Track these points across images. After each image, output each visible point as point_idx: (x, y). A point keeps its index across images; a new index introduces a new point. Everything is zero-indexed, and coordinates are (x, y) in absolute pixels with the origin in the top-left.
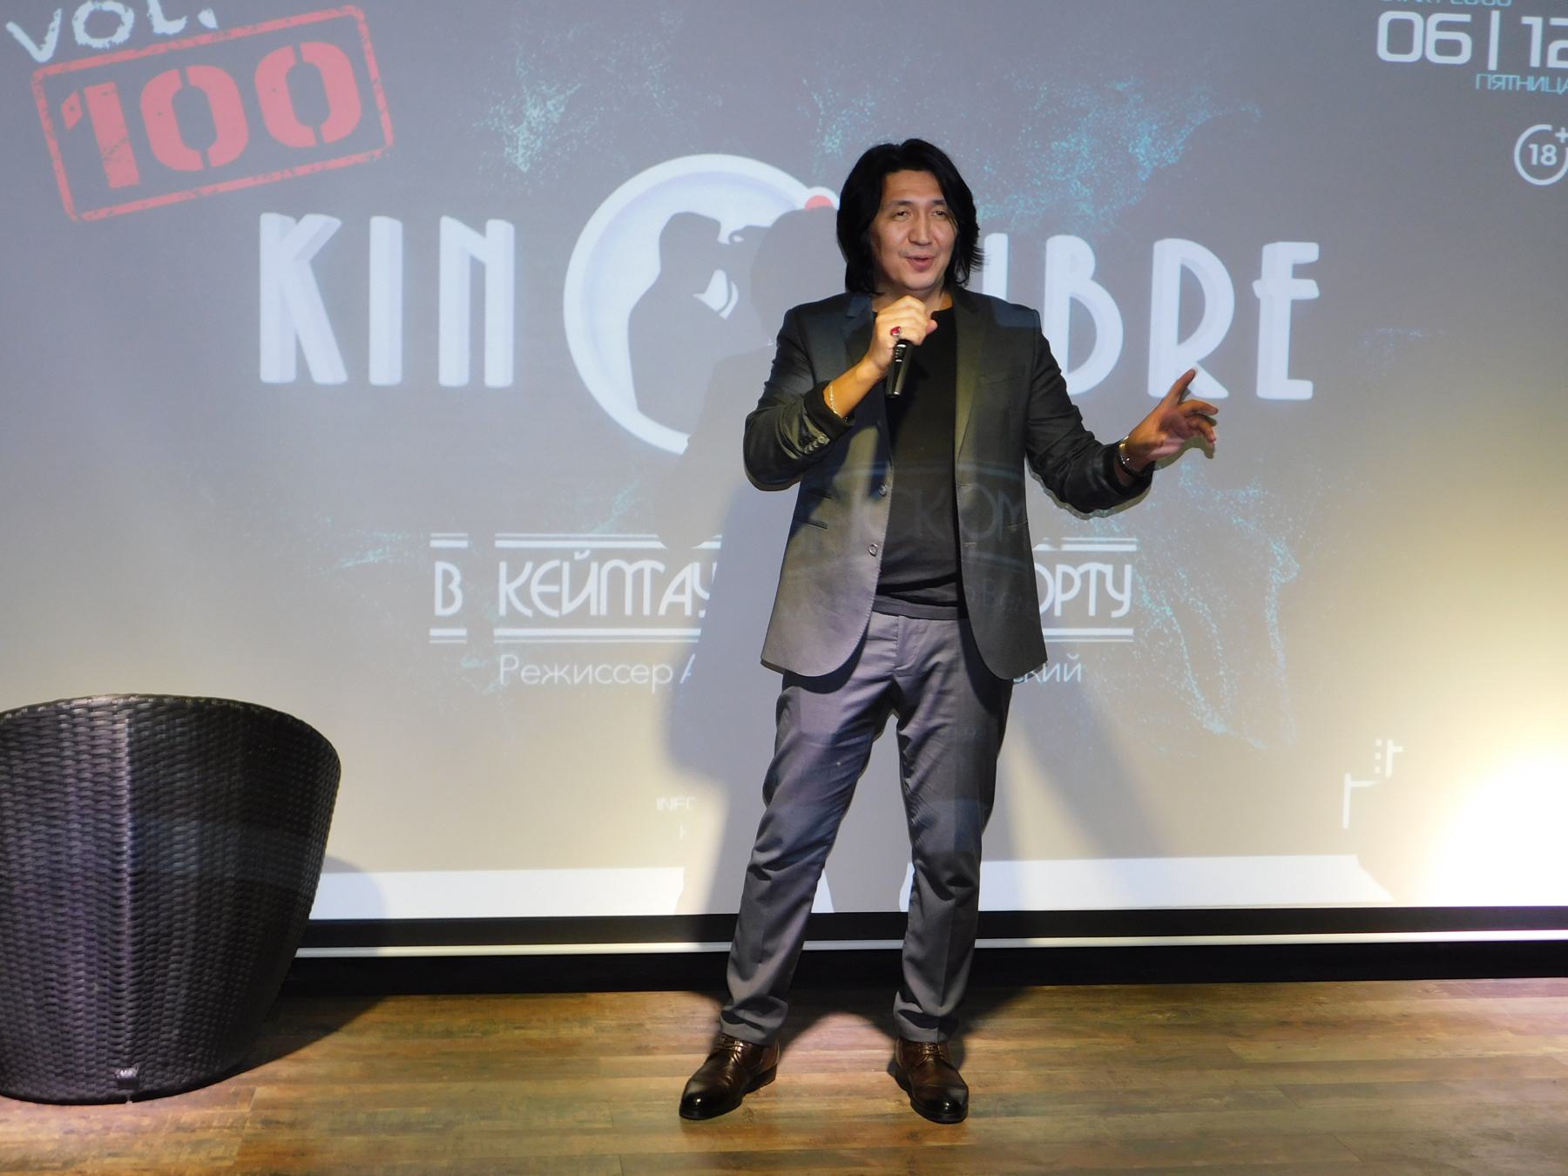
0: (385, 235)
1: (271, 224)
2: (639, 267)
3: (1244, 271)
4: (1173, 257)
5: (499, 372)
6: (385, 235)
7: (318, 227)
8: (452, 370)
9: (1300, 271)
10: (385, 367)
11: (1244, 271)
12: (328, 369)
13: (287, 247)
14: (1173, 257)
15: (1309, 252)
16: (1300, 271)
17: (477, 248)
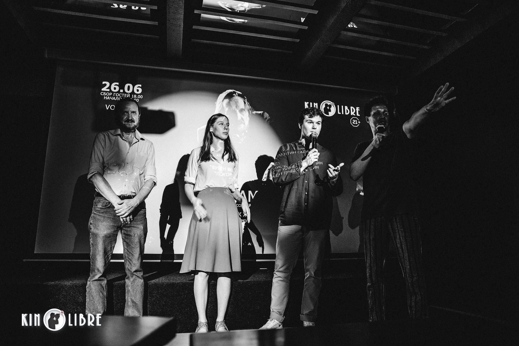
0: (311, 103)
2: (324, 106)
3: (356, 109)
4: (351, 107)
6: (311, 103)
7: (308, 103)
11: (356, 109)
14: (351, 107)
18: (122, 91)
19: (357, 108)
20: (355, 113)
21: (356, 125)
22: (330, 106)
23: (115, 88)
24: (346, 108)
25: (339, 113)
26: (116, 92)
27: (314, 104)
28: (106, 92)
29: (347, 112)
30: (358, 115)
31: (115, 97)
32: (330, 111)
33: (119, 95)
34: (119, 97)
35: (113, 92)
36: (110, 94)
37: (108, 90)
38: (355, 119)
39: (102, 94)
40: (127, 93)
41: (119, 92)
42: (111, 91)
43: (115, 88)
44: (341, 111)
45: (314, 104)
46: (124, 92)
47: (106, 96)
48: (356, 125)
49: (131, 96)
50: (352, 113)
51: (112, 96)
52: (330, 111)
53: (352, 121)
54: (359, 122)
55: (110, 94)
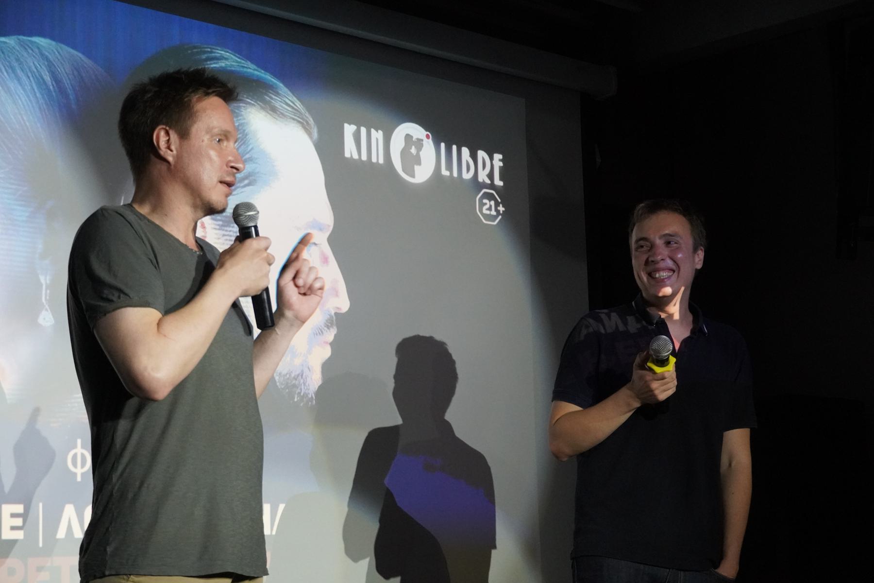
0: (363, 130)
1: (346, 125)
3: (492, 159)
4: (481, 154)
5: (381, 161)
6: (363, 130)
7: (353, 128)
8: (374, 160)
9: (500, 160)
10: (364, 157)
11: (492, 159)
12: (356, 156)
13: (349, 129)
15: (501, 157)
16: (500, 160)
17: (377, 135)
19: (498, 157)
20: (491, 176)
21: (493, 218)
22: (419, 144)
24: (465, 151)
25: (445, 173)
27: (373, 131)
29: (468, 169)
30: (498, 183)
32: (419, 163)
38: (490, 197)
44: (449, 167)
45: (373, 131)
48: (493, 218)
50: (483, 177)
52: (419, 163)
53: (482, 205)
54: (501, 209)
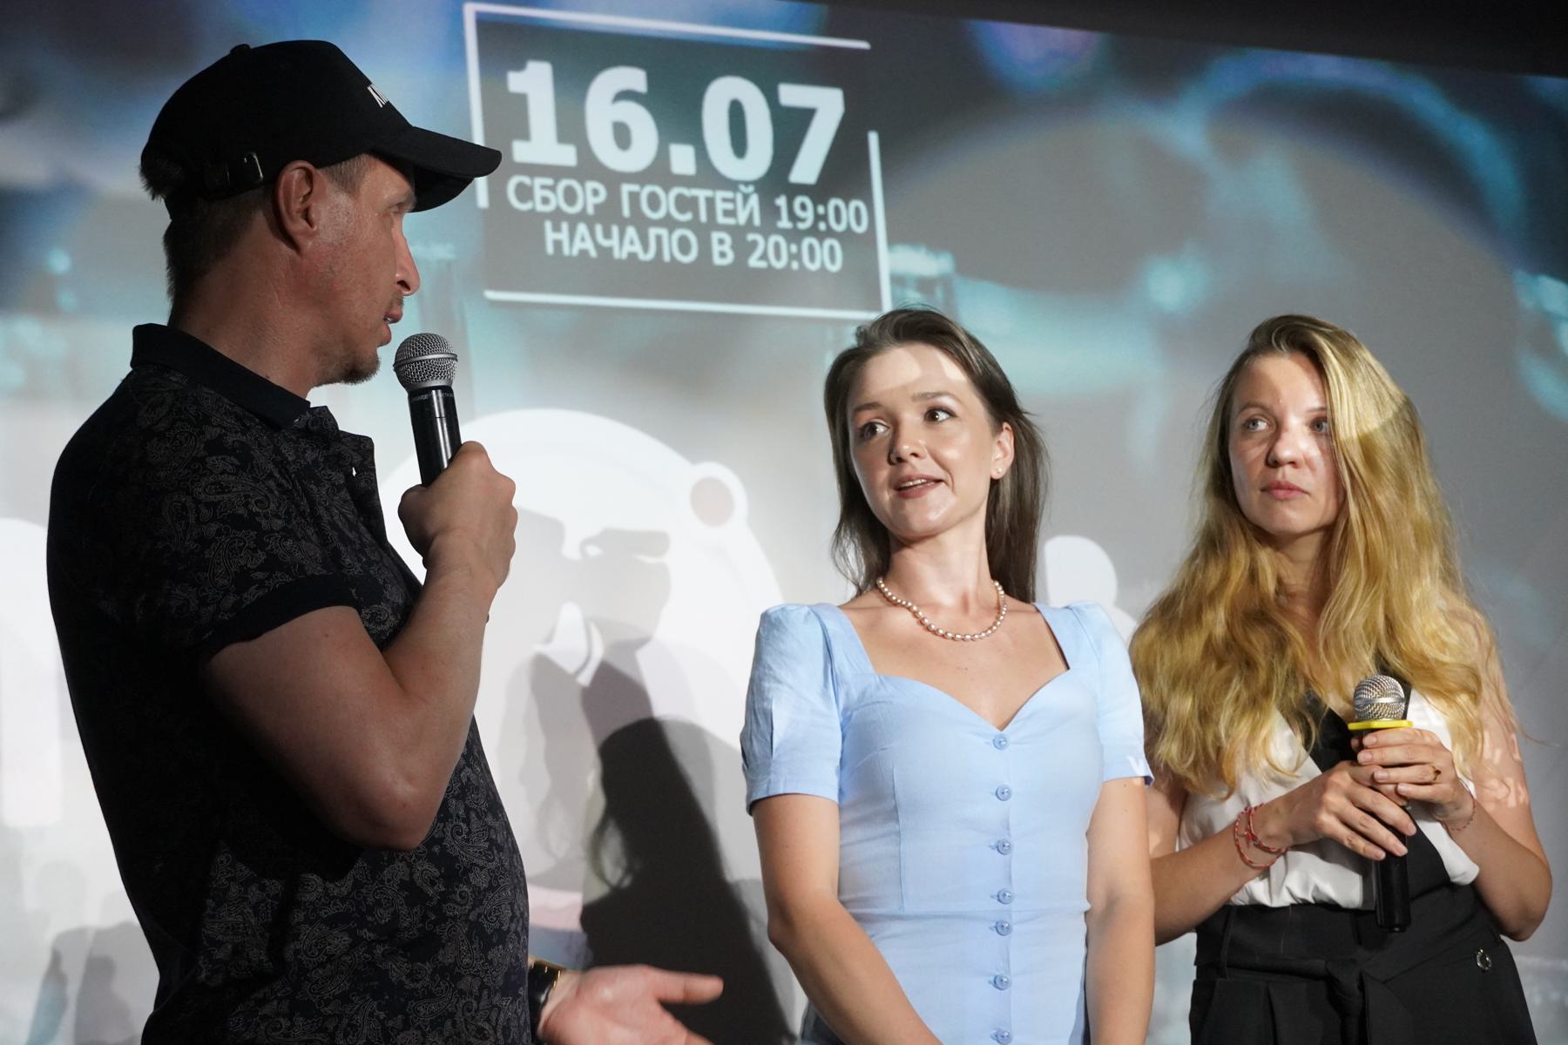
18: (683, 159)
23: (622, 135)
26: (640, 178)
28: (557, 172)
31: (643, 225)
33: (668, 201)
34: (669, 223)
35: (612, 179)
36: (591, 195)
37: (567, 156)
39: (525, 193)
40: (732, 185)
41: (659, 172)
42: (589, 167)
43: (622, 135)
46: (708, 174)
47: (557, 217)
49: (769, 211)
51: (608, 215)
55: (591, 195)
